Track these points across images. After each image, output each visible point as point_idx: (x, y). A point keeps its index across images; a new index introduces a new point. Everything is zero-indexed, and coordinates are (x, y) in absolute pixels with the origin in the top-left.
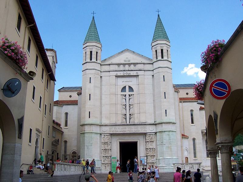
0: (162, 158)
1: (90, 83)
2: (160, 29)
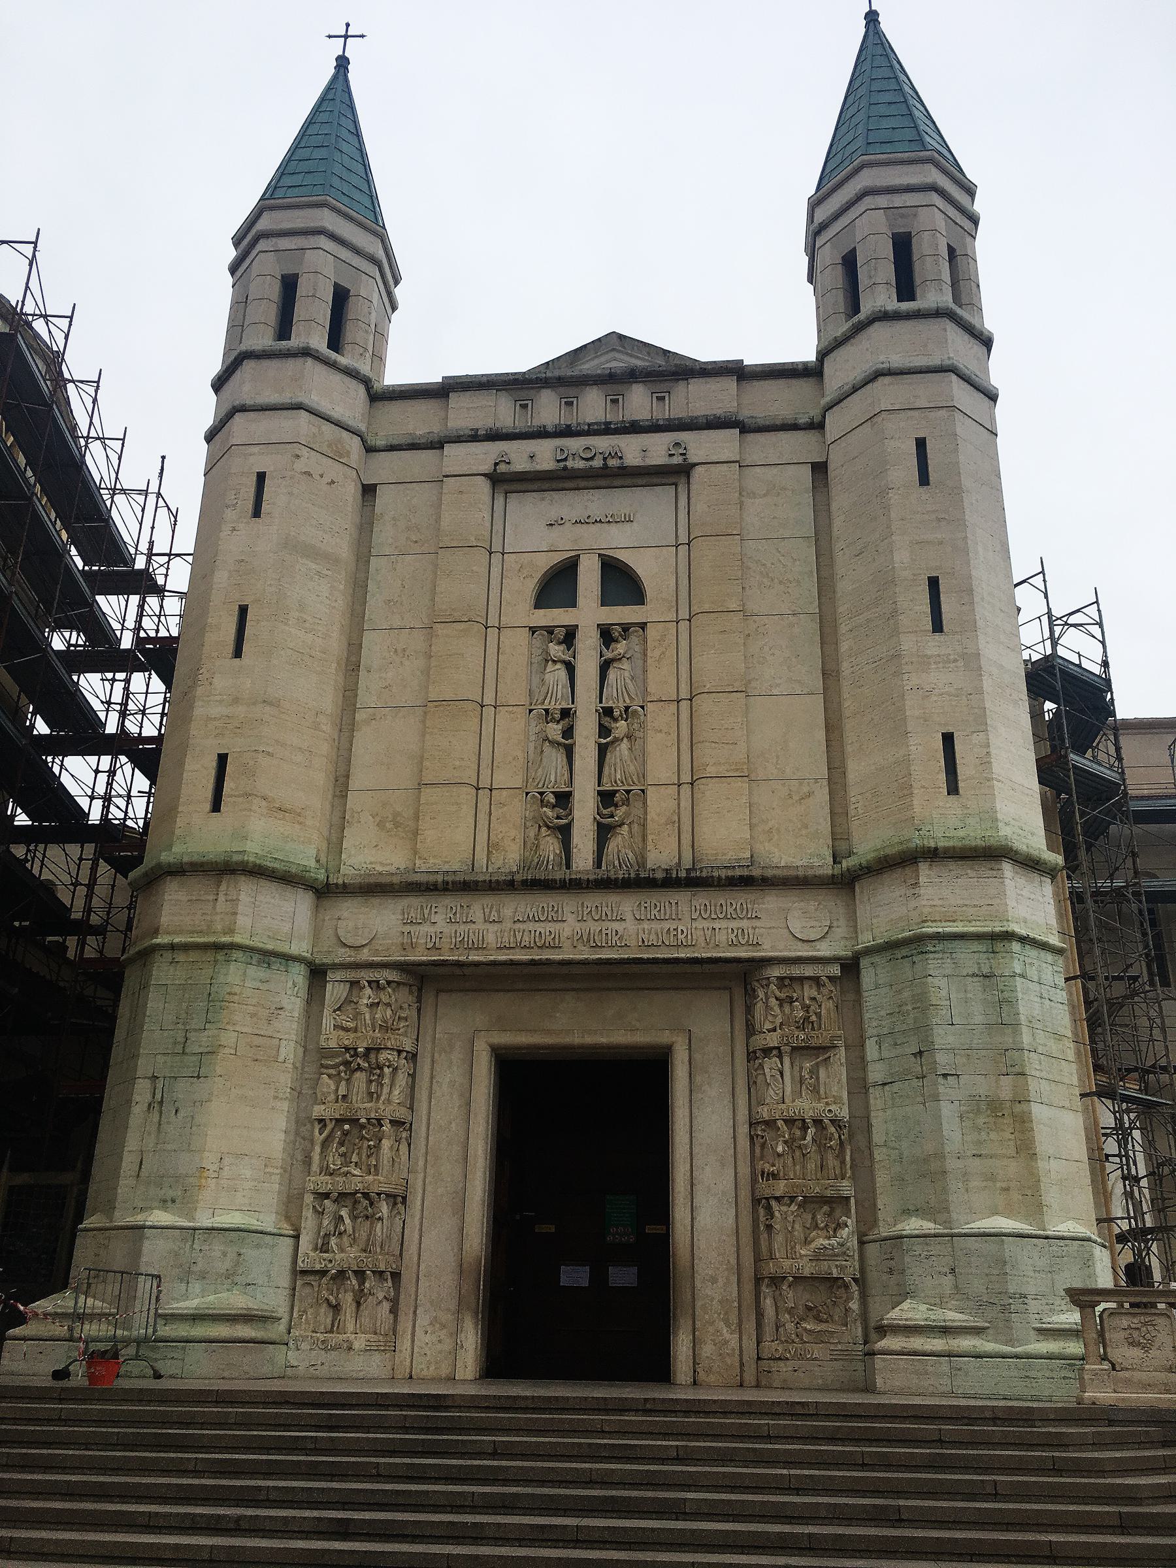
0: (928, 1226)
1: (257, 513)
2: (888, 97)
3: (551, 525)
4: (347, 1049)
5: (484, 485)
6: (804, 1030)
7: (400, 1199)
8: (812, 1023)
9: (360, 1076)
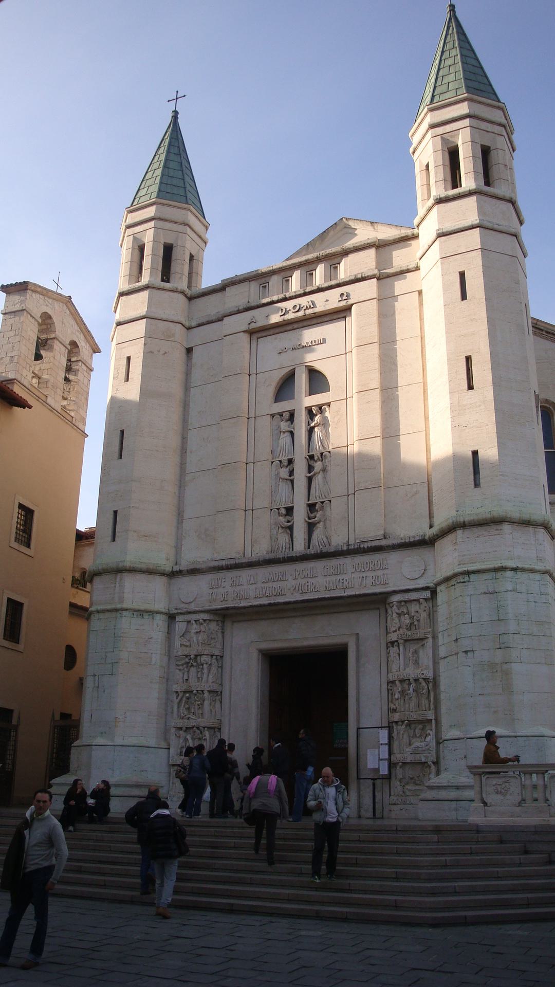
3: (280, 353)
4: (187, 656)
5: (245, 338)
6: (411, 629)
7: (216, 730)
8: (415, 625)
9: (193, 670)
